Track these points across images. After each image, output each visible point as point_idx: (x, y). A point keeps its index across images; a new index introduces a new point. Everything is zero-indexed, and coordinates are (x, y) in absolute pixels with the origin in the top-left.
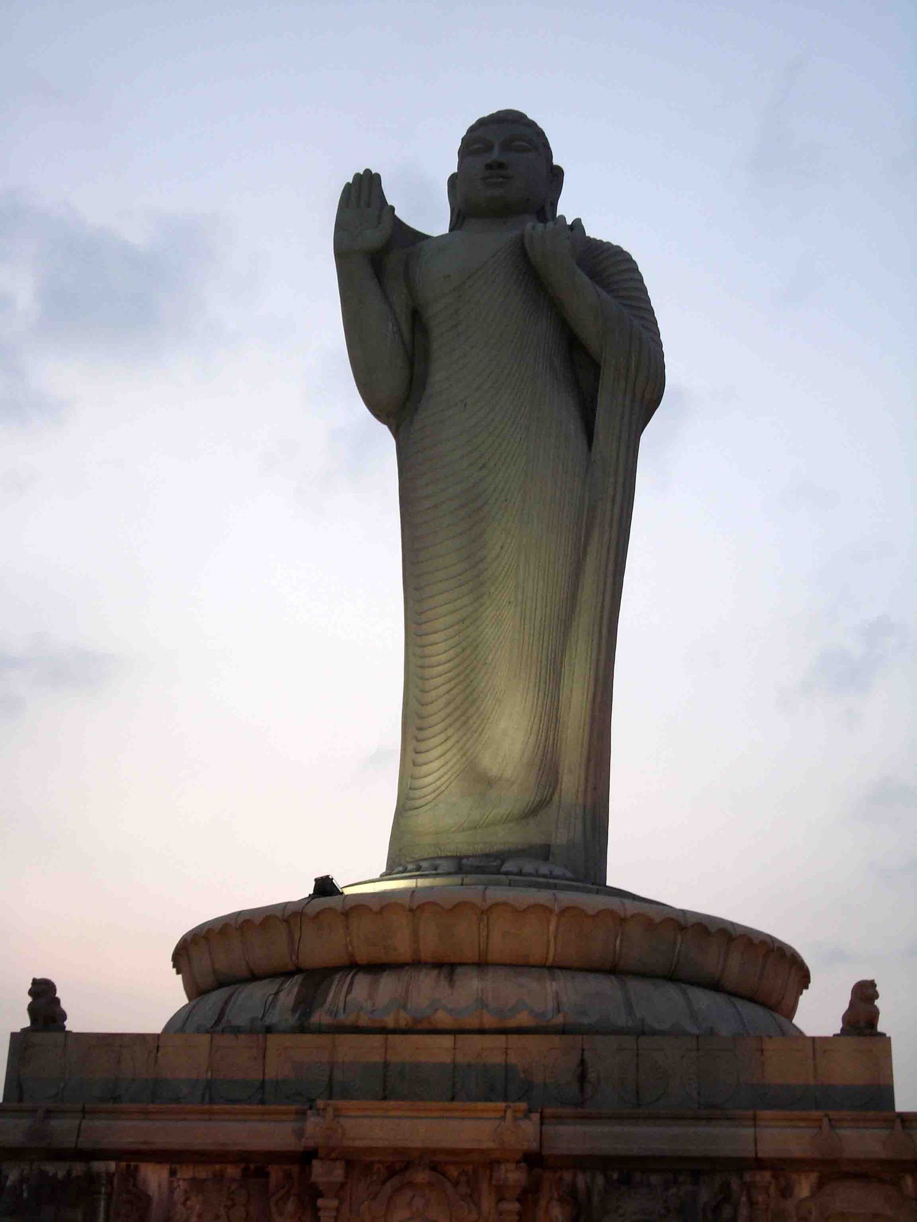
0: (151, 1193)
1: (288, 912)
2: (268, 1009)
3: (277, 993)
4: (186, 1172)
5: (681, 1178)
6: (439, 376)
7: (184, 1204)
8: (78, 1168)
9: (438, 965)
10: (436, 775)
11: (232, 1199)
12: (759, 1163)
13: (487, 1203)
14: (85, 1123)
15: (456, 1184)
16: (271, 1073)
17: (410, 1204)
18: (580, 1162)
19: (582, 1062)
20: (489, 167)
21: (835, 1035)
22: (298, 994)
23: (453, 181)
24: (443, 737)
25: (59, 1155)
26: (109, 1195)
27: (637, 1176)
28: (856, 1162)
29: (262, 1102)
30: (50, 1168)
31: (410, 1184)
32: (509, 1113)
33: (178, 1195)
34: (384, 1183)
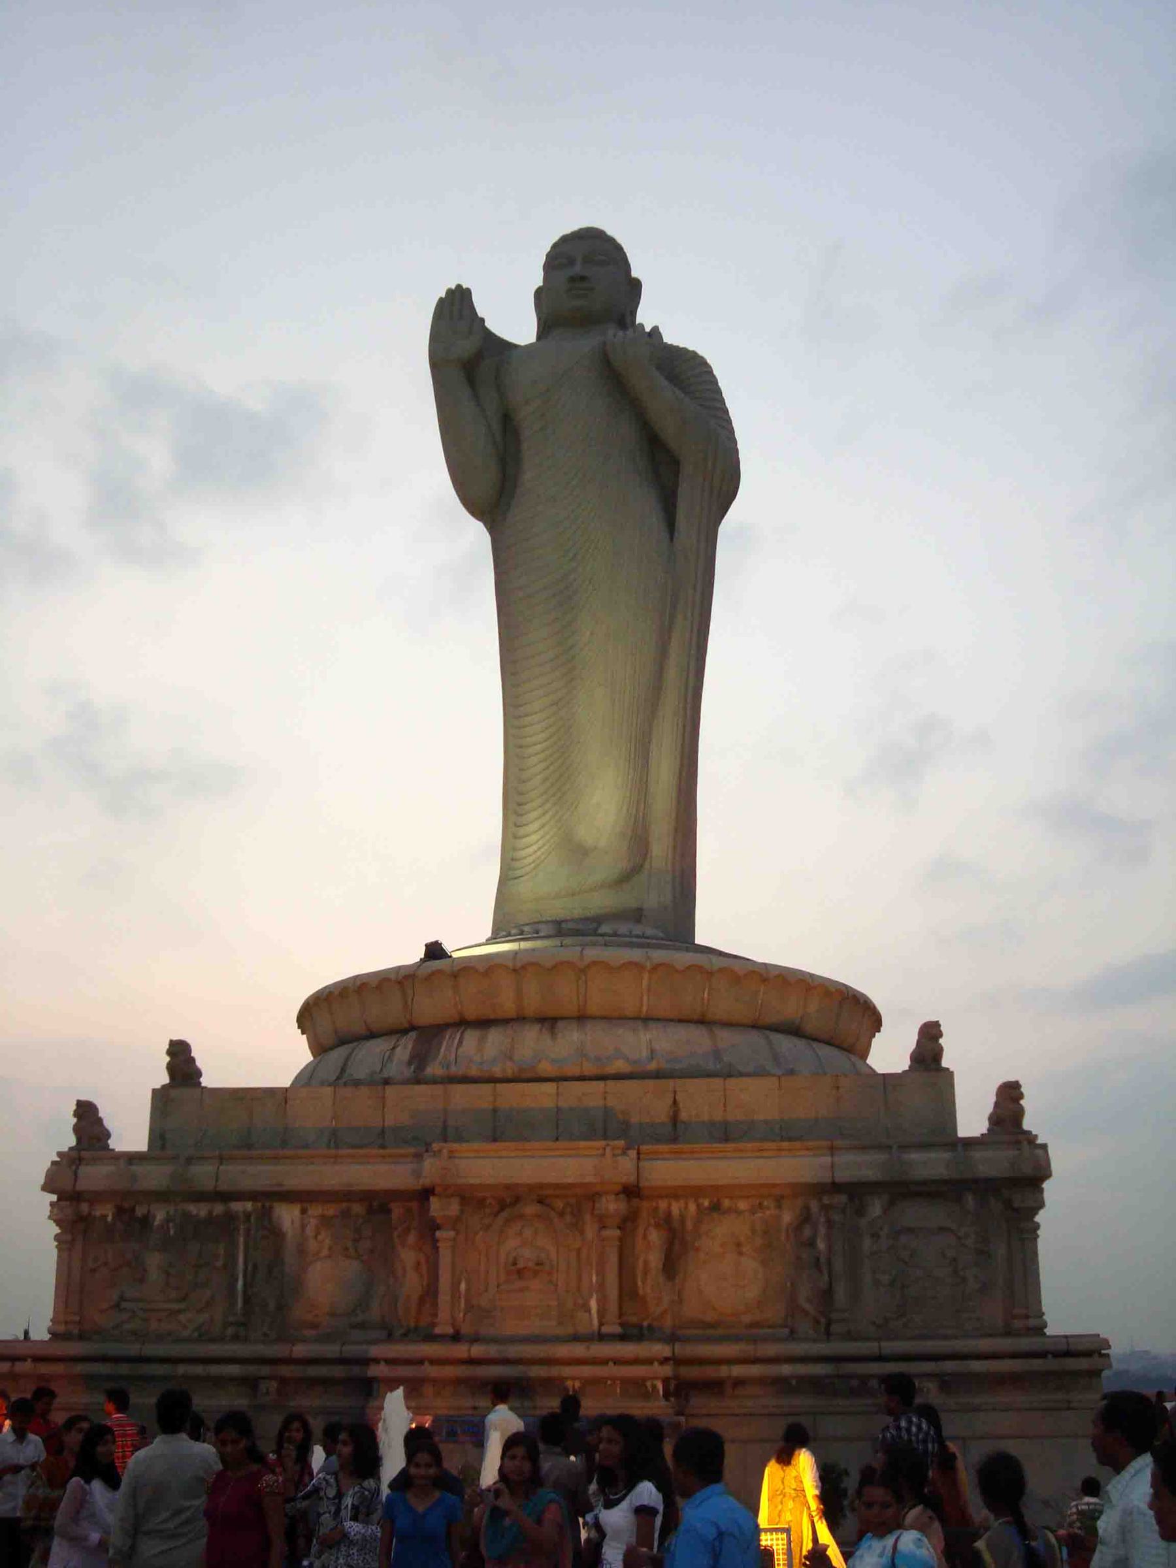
0: (284, 1230)
1: (402, 973)
3: (394, 1048)
4: (315, 1210)
6: (528, 476)
7: (316, 1237)
8: (219, 1209)
10: (535, 847)
12: (835, 1187)
13: (590, 1231)
15: (561, 1214)
16: (390, 1121)
17: (520, 1234)
19: (675, 1102)
20: (572, 279)
22: (413, 1048)
23: (539, 294)
24: (540, 811)
25: (200, 1197)
27: (726, 1203)
28: (924, 1183)
29: (383, 1147)
30: (192, 1208)
31: (521, 1217)
32: (608, 1150)
33: (310, 1231)
34: (496, 1215)
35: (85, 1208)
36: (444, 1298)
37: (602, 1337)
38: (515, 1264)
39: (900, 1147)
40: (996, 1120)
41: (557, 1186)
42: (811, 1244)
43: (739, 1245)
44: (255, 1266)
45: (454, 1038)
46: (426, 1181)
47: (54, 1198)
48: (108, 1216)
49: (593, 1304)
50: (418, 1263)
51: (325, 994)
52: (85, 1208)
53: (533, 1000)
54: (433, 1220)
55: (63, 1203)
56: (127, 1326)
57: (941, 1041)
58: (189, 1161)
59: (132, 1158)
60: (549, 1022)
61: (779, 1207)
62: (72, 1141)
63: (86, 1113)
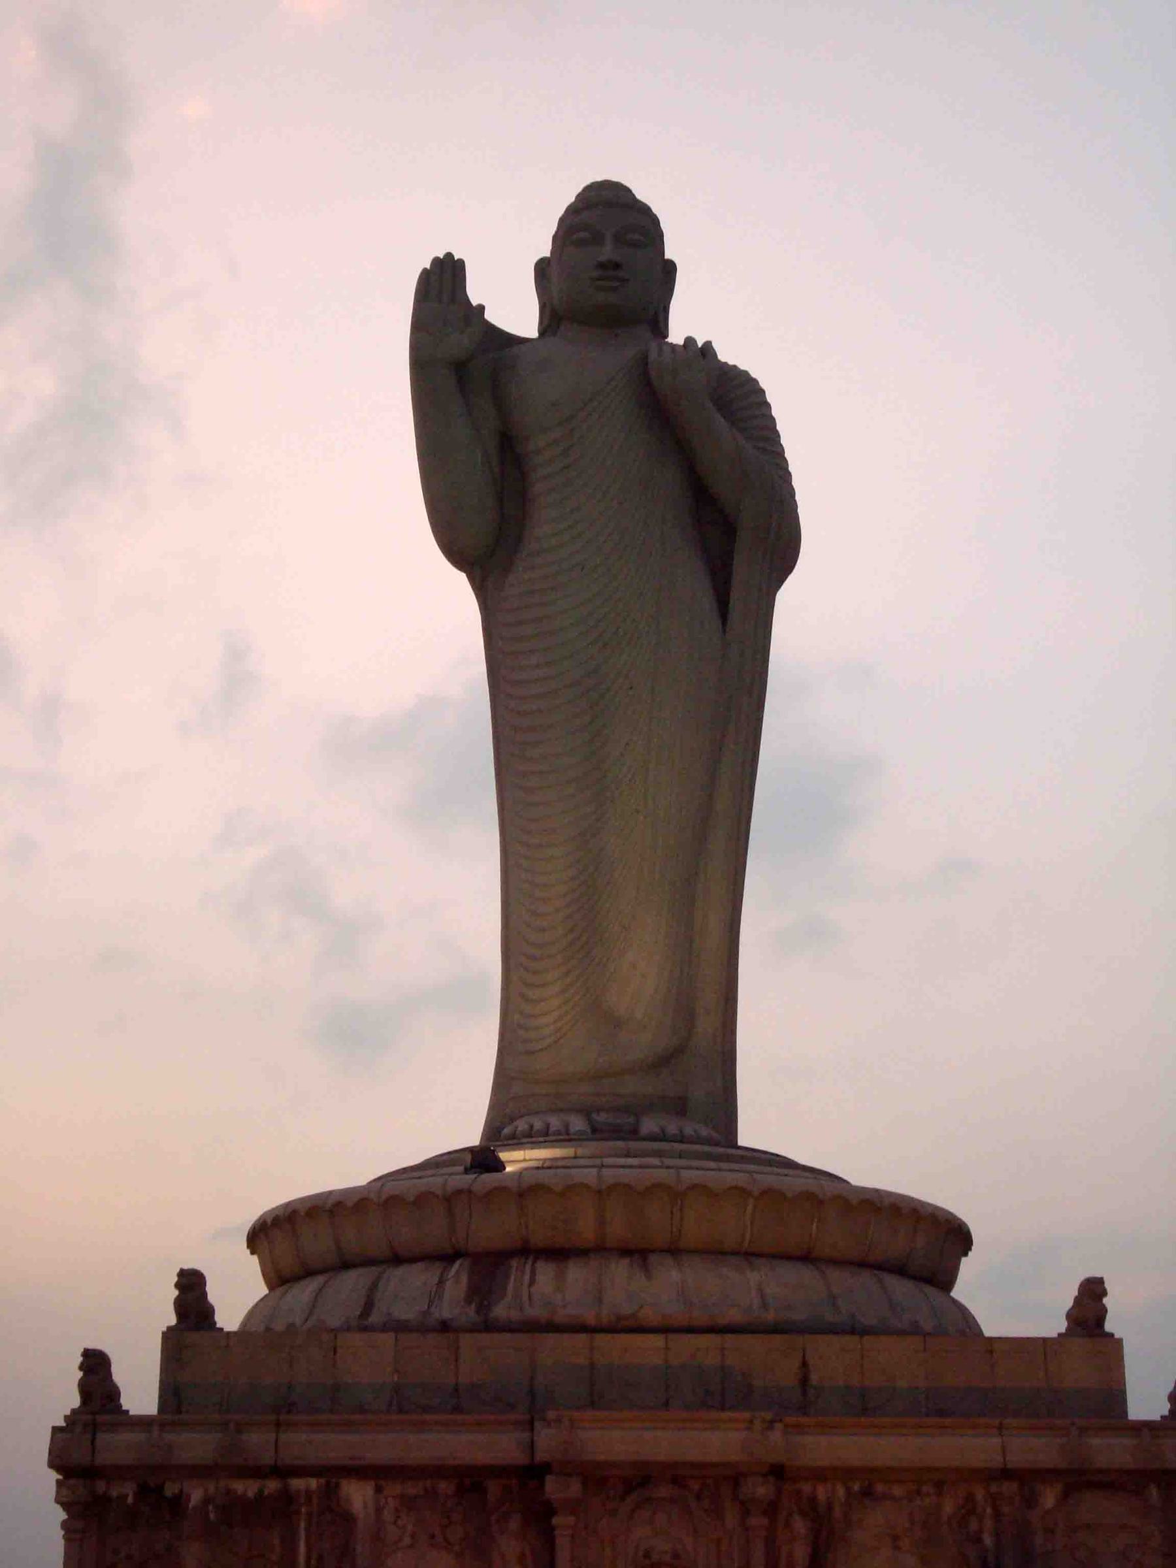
2: (435, 1298)
3: (441, 1282)
4: (394, 1489)
5: (925, 1489)
7: (395, 1523)
9: (626, 1252)
11: (448, 1517)
12: (1006, 1474)
13: (731, 1517)
14: (283, 1437)
15: (698, 1497)
18: (820, 1475)
19: (804, 1364)
20: (602, 266)
21: (1060, 1335)
23: (542, 268)
25: (257, 1472)
26: (309, 1515)
27: (880, 1488)
29: (457, 1409)
30: (239, 1486)
33: (388, 1515)
34: (623, 1499)
35: (101, 1487)
38: (647, 1555)
41: (693, 1465)
43: (895, 1538)
44: (320, 1558)
45: (523, 1272)
46: (541, 1456)
48: (128, 1495)
51: (330, 1202)
52: (101, 1487)
53: (618, 1229)
55: (72, 1482)
57: (1105, 1300)
59: (143, 1422)
61: (940, 1494)
62: (75, 1401)
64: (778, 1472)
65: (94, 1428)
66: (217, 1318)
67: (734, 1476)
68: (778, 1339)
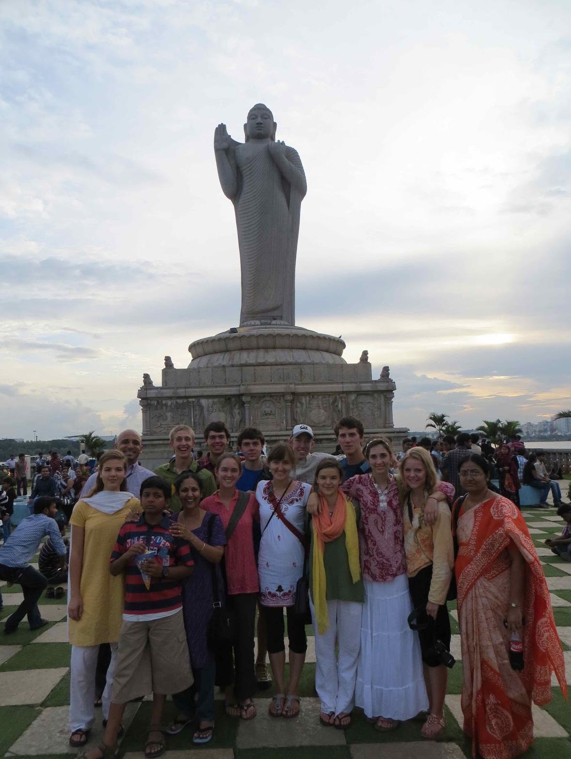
8: (185, 401)
9: (263, 348)
12: (343, 392)
17: (265, 405)
20: (257, 124)
23: (245, 126)
30: (179, 401)
36: (247, 421)
37: (287, 430)
38: (265, 412)
39: (360, 382)
40: (382, 376)
42: (337, 406)
46: (242, 392)
47: (140, 399)
49: (284, 422)
50: (239, 413)
54: (243, 402)
56: (163, 431)
58: (177, 388)
59: (157, 388)
60: (266, 348)
62: (143, 384)
63: (146, 377)
64: (293, 394)
65: (146, 389)
66: (174, 366)
67: (283, 395)
68: (295, 366)
